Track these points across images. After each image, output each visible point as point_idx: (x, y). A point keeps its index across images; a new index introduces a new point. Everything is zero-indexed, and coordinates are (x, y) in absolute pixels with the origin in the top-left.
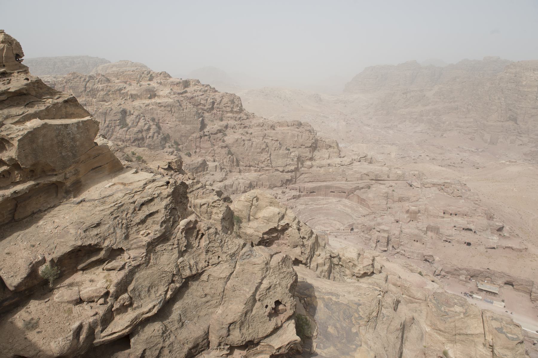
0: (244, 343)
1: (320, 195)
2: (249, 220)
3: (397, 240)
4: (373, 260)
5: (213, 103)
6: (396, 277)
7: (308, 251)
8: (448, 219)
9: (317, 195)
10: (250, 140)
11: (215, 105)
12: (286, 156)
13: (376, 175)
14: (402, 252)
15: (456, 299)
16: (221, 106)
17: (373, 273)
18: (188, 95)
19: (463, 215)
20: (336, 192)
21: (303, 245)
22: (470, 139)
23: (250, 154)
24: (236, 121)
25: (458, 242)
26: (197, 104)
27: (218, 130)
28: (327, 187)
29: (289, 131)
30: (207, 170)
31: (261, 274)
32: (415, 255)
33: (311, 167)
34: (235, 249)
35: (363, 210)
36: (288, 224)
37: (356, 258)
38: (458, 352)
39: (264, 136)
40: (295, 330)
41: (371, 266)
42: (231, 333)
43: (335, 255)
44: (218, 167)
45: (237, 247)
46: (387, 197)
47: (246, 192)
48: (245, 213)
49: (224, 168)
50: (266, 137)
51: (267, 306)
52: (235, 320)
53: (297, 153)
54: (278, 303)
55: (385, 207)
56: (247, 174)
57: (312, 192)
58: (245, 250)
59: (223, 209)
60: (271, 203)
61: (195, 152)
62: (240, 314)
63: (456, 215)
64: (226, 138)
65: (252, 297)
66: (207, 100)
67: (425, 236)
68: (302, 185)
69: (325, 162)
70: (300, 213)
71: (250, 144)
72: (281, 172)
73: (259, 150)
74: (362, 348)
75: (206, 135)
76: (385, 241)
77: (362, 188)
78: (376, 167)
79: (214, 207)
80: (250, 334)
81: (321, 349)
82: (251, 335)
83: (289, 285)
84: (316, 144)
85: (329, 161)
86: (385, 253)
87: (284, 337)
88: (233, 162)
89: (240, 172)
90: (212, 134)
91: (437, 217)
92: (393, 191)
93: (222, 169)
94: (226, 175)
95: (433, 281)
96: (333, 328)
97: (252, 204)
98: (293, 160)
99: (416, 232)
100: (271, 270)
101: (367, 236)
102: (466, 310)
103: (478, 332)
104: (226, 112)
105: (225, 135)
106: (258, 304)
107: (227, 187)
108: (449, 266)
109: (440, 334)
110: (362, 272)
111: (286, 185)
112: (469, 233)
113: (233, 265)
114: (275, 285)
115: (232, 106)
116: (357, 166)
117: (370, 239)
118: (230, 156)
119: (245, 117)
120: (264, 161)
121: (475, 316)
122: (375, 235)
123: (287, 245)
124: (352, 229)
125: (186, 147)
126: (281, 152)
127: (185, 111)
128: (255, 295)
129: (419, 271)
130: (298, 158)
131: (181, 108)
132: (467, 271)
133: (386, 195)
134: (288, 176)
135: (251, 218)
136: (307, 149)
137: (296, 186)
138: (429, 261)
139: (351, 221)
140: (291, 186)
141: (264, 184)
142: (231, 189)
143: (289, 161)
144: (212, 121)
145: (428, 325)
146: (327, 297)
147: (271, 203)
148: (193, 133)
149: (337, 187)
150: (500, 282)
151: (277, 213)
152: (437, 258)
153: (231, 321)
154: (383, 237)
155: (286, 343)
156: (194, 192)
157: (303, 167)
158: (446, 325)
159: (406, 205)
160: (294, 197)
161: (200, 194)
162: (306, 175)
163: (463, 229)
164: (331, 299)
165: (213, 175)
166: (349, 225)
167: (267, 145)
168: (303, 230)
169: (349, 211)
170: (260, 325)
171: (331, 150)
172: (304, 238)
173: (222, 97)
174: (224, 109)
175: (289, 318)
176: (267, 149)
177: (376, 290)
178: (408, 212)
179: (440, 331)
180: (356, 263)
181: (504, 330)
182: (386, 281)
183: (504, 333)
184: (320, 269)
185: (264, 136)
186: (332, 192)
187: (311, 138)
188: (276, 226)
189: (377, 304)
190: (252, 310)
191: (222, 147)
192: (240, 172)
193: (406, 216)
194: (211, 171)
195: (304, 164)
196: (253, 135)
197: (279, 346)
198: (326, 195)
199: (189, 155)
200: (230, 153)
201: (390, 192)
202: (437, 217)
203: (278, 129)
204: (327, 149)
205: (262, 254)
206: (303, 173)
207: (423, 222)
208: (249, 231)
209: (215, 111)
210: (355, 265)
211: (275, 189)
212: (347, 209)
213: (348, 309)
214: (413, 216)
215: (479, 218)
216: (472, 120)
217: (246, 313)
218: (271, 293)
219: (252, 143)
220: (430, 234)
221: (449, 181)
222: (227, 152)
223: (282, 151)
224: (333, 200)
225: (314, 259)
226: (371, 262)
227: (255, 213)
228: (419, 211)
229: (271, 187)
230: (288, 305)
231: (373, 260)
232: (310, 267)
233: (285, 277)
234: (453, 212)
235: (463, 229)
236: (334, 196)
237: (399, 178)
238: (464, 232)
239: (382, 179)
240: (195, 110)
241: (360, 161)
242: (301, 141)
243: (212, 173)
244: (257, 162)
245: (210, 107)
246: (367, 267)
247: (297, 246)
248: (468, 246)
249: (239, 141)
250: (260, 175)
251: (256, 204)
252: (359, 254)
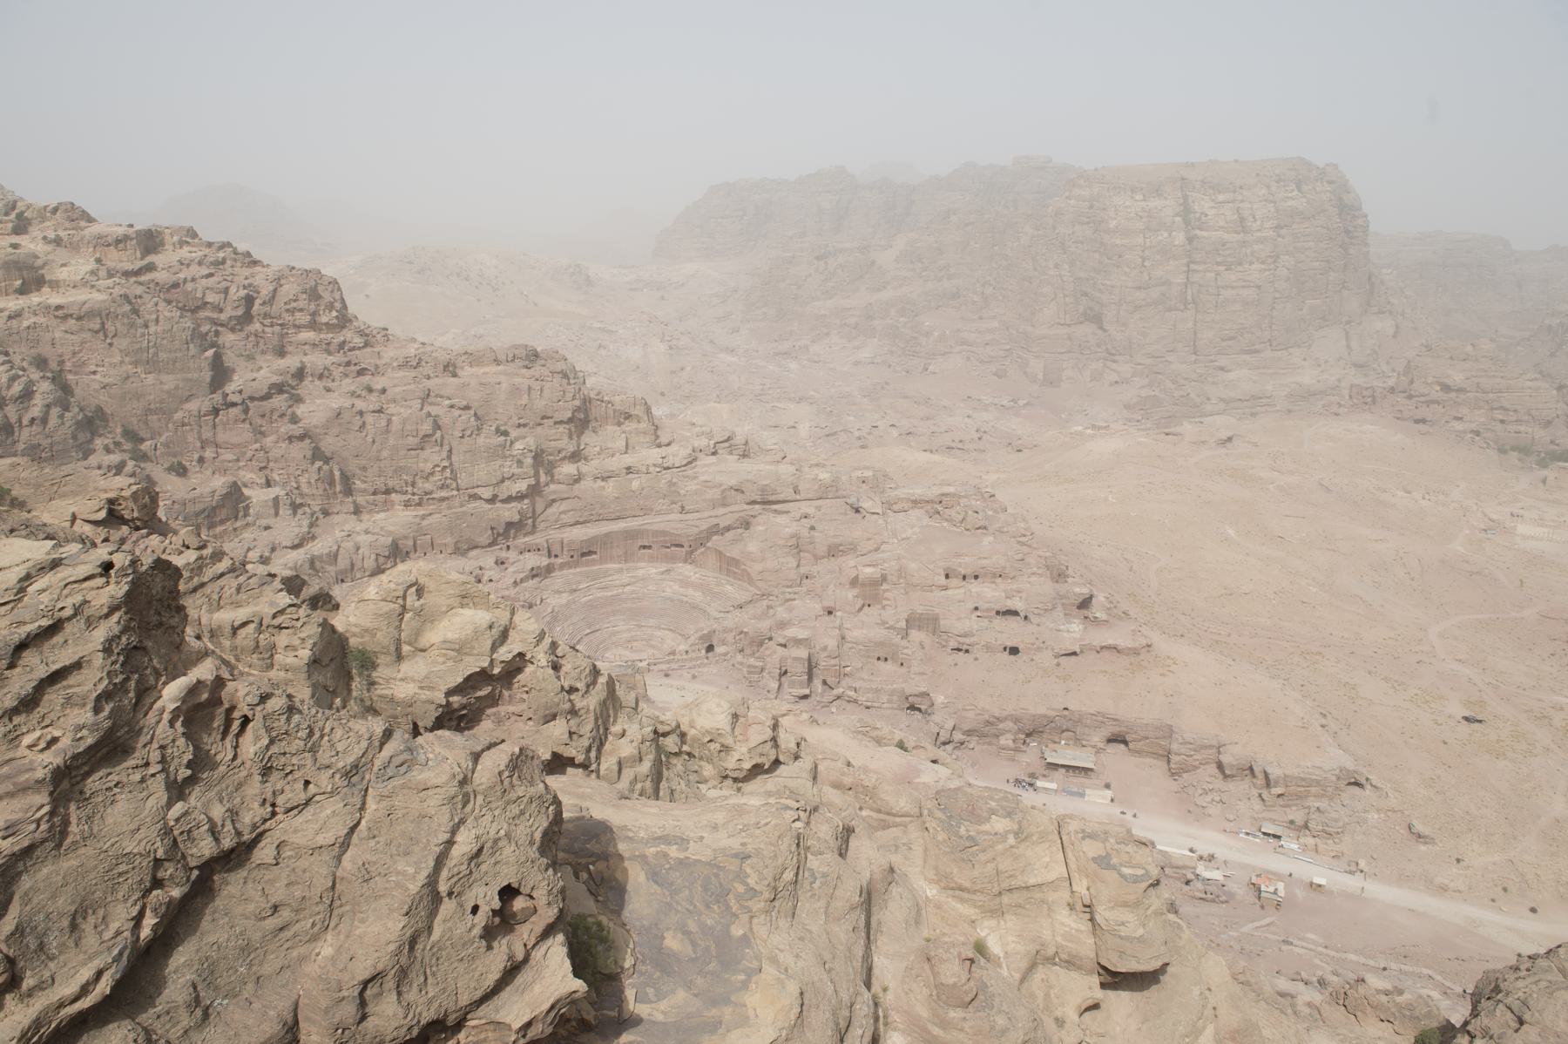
0: (415, 1032)
1: (611, 559)
2: (400, 657)
3: (833, 662)
4: (775, 727)
5: (249, 301)
6: (840, 764)
7: (587, 728)
8: (957, 591)
9: (602, 561)
10: (380, 411)
11: (256, 307)
12: (500, 452)
13: (763, 490)
14: (852, 693)
15: (992, 799)
16: (275, 310)
17: (777, 763)
18: (161, 276)
19: (994, 576)
21: (573, 712)
22: (995, 374)
23: (385, 454)
24: (330, 353)
25: (988, 648)
26: (191, 305)
27: (273, 386)
28: (630, 535)
29: (503, 378)
30: (246, 515)
31: (447, 816)
32: (885, 698)
33: (578, 479)
34: (358, 751)
35: (734, 591)
36: (521, 655)
37: (728, 728)
38: (1010, 938)
39: (426, 397)
40: (568, 964)
41: (769, 744)
42: (370, 1009)
43: (667, 728)
44: (284, 501)
45: (364, 744)
46: (797, 547)
47: (383, 571)
48: (383, 638)
49: (302, 505)
50: (431, 400)
51: (475, 909)
52: (380, 967)
53: (531, 442)
54: (508, 893)
55: (793, 575)
56: (382, 515)
57: (586, 552)
58: (389, 749)
59: (312, 630)
60: (464, 597)
61: (201, 460)
62: (392, 947)
63: (976, 577)
64: (301, 410)
65: (426, 891)
66: (226, 291)
67: (904, 643)
68: (555, 535)
69: (617, 463)
70: (555, 617)
71: (384, 423)
72: (488, 501)
73: (412, 441)
74: (763, 976)
75: (234, 405)
76: (801, 668)
77: (728, 529)
78: (761, 467)
79: (280, 628)
80: (430, 1002)
81: (650, 1002)
82: (436, 1005)
83: (538, 836)
84: (587, 415)
85: (628, 460)
86: (804, 704)
87: (537, 988)
88: (332, 483)
89: (357, 511)
90: (252, 399)
91: (930, 587)
92: (813, 528)
93: (295, 507)
94: (311, 525)
95: (934, 762)
96: (680, 936)
97: (404, 607)
98: (520, 463)
99: (880, 634)
100: (480, 799)
101: (752, 661)
102: (1019, 823)
103: (1052, 876)
104: (295, 326)
105: (299, 400)
106: (447, 907)
107: (318, 564)
108: (971, 715)
109: (961, 900)
110: (747, 765)
112: (1012, 622)
113: (358, 801)
114: (496, 841)
115: (312, 307)
116: (708, 468)
117: (762, 670)
118: (318, 464)
119: (358, 341)
120: (432, 474)
121: (1043, 836)
122: (774, 656)
123: (525, 717)
124: (710, 648)
125: (166, 445)
126: (481, 440)
127: (152, 329)
128: (436, 882)
129: (897, 738)
130: (535, 458)
131: (140, 321)
132: (1016, 720)
133: (793, 541)
134: (510, 512)
135: (406, 648)
136: (561, 428)
137: (538, 539)
138: (919, 710)
139: (705, 626)
140: (522, 541)
141: (438, 541)
142: (331, 569)
143: (510, 468)
144: (250, 358)
145: (931, 881)
146: (653, 850)
147: (464, 597)
148: (188, 399)
149: (657, 533)
150: (1097, 738)
151: (485, 624)
152: (940, 699)
153: (367, 975)
155: (546, 1006)
156: (208, 590)
157: (552, 481)
158: (976, 873)
159: (850, 565)
160: (534, 574)
161: (229, 592)
162: (564, 506)
163: (998, 613)
164: (666, 855)
165: (267, 528)
167: (435, 422)
168: (567, 667)
169: (697, 596)
170: (461, 967)
171: (630, 426)
172: (572, 690)
173: (278, 281)
174: (288, 318)
175: (548, 932)
176: (438, 434)
177: (787, 808)
178: (854, 582)
179: (962, 889)
180: (729, 741)
181: (1114, 861)
182: (815, 778)
183: (1114, 868)
184: (628, 774)
185: (426, 397)
187: (569, 396)
188: (486, 665)
189: (794, 847)
190: (430, 928)
191: (290, 439)
192: (357, 511)
193: (850, 594)
194: (258, 516)
195: (556, 471)
196: (390, 393)
197: (526, 1019)
198: (627, 557)
199: (181, 471)
200: (317, 454)
201: (805, 533)
202: (930, 587)
203: (467, 372)
204: (619, 424)
205: (446, 753)
206: (554, 501)
207: (897, 607)
208: (403, 691)
209: (257, 326)
210: (725, 749)
211: (473, 553)
212: (690, 591)
213: (716, 876)
214: (870, 591)
215: (1033, 579)
216: (996, 324)
217: (413, 942)
218: (484, 867)
219: (389, 422)
220: (916, 635)
221: (951, 490)
222: (309, 454)
223: (487, 439)
224: (649, 570)
225: (607, 747)
226: (769, 733)
227: (418, 633)
228: (884, 579)
229: (461, 550)
230: (541, 895)
231: (775, 727)
232: (598, 771)
233: (522, 813)
234: (968, 571)
235: (998, 613)
236: (652, 559)
237: (826, 492)
238: (999, 622)
239: (780, 497)
240: (188, 323)
241: (714, 454)
242: (540, 404)
243: (264, 522)
244: (410, 479)
245: (240, 312)
246: (759, 750)
247: (554, 717)
248: (1013, 657)
249: (346, 416)
250: (423, 517)
251: (417, 604)
252: (735, 716)
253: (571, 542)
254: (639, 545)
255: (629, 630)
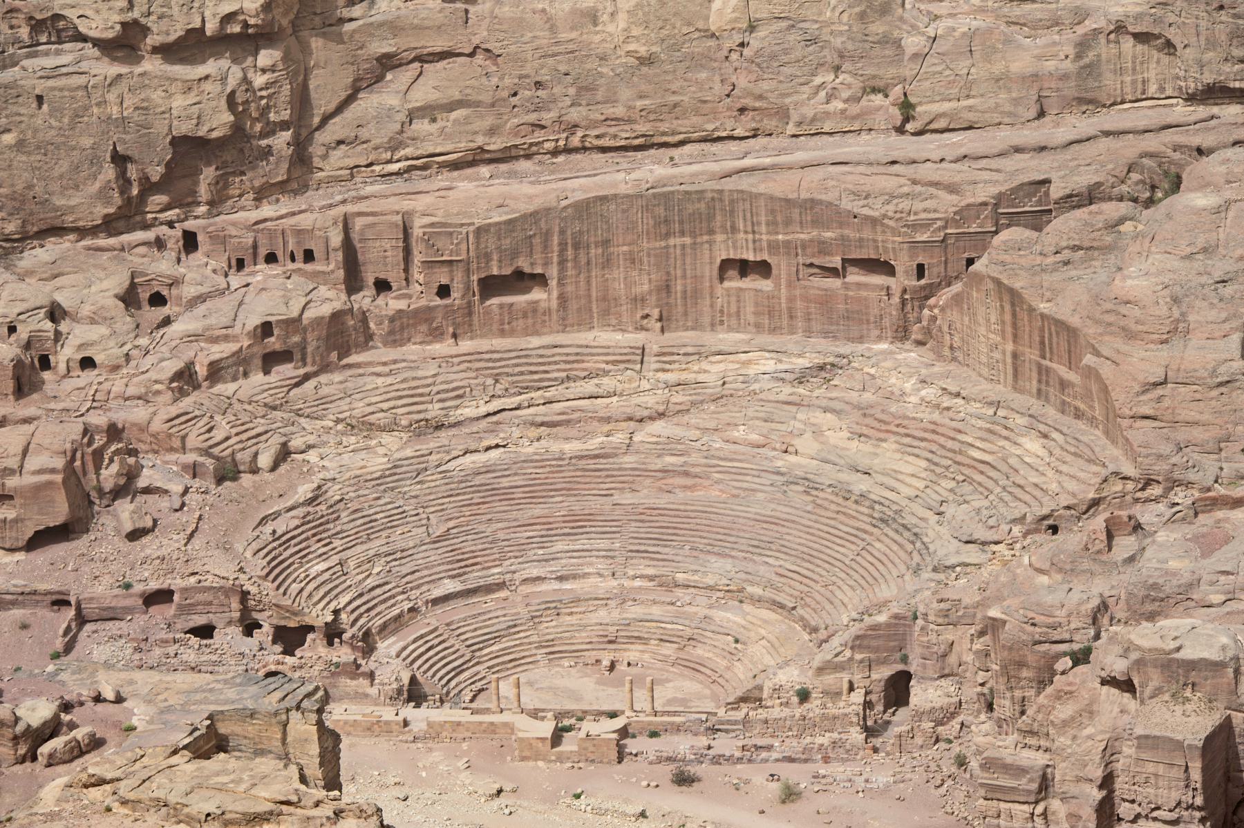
1: (607, 310)
9: (570, 314)
20: (781, 265)
28: (679, 214)
35: (1049, 461)
57: (501, 277)
68: (382, 201)
70: (318, 519)
77: (1090, 196)
111: (185, 202)
124: (898, 690)
134: (194, 98)
137: (313, 214)
139: (897, 590)
140: (243, 217)
149: (788, 210)
154: (1146, 742)
160: (273, 347)
162: (431, 85)
166: (858, 643)
169: (900, 471)
186: (744, 267)
206: (388, 63)
211: (40, 255)
212: (888, 456)
224: (747, 359)
236: (772, 318)
253: (441, 230)
254: (716, 256)
255: (623, 598)
